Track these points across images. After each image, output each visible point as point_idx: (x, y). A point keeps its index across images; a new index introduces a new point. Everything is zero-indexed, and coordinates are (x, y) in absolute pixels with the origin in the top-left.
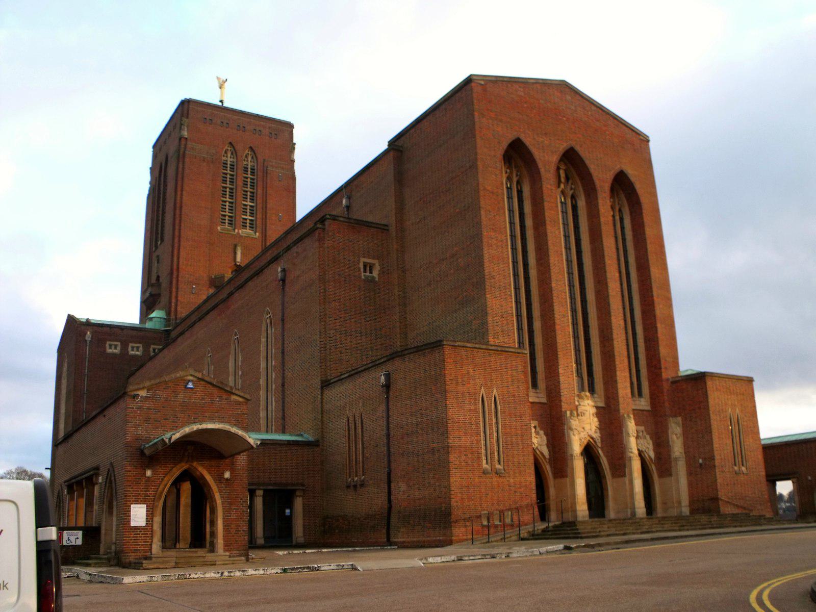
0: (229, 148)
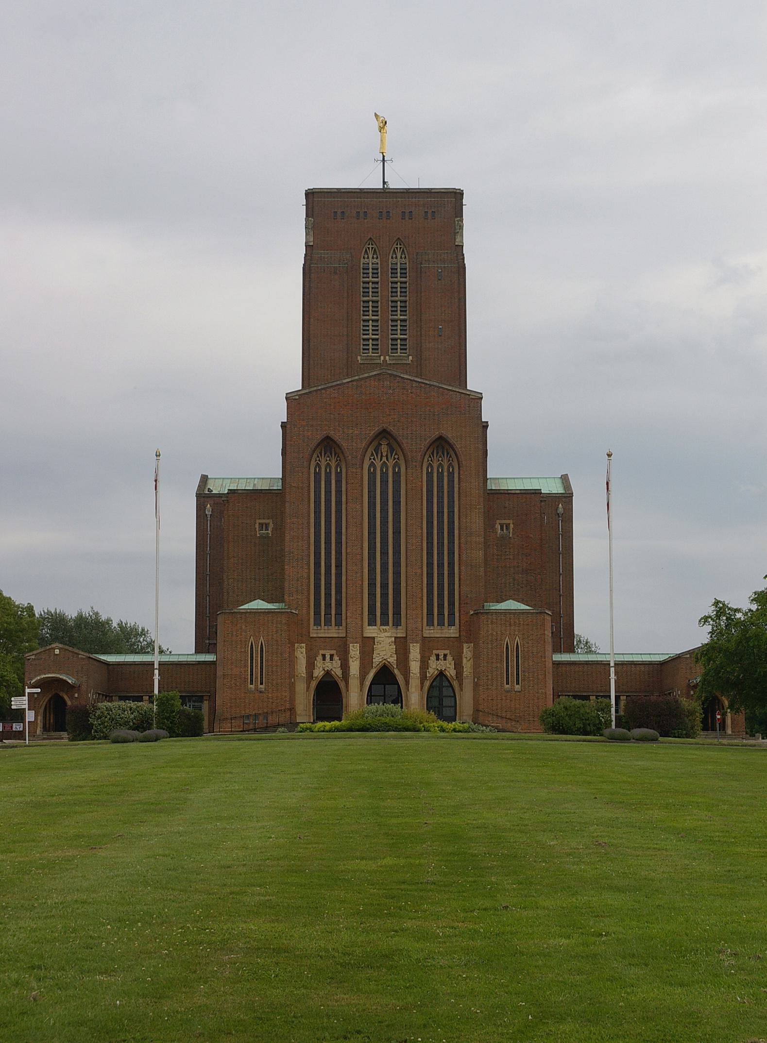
0: (370, 246)
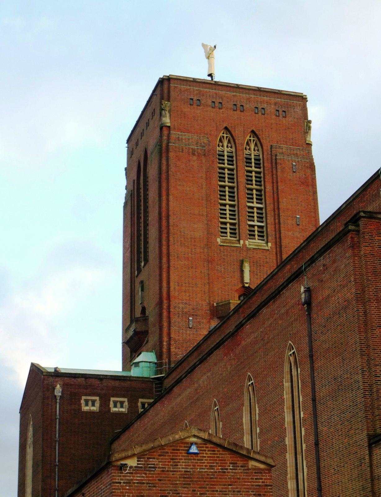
0: (225, 135)
